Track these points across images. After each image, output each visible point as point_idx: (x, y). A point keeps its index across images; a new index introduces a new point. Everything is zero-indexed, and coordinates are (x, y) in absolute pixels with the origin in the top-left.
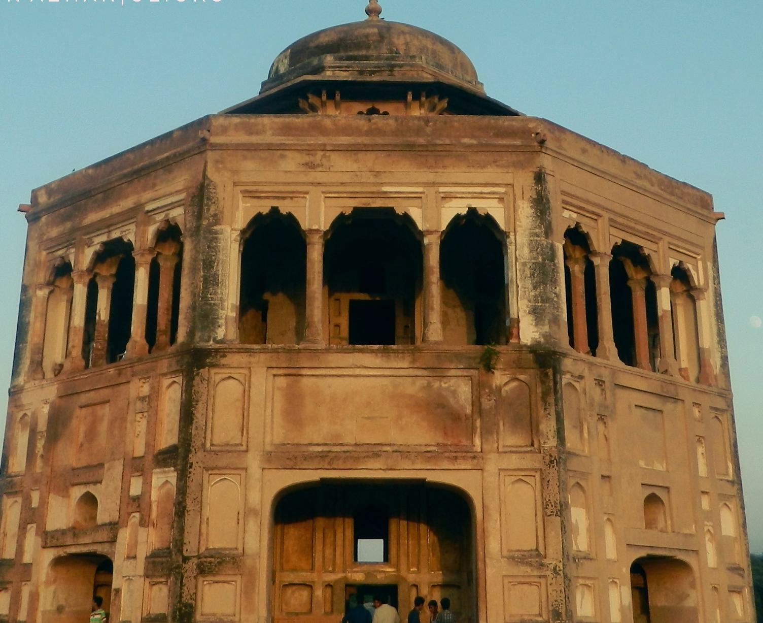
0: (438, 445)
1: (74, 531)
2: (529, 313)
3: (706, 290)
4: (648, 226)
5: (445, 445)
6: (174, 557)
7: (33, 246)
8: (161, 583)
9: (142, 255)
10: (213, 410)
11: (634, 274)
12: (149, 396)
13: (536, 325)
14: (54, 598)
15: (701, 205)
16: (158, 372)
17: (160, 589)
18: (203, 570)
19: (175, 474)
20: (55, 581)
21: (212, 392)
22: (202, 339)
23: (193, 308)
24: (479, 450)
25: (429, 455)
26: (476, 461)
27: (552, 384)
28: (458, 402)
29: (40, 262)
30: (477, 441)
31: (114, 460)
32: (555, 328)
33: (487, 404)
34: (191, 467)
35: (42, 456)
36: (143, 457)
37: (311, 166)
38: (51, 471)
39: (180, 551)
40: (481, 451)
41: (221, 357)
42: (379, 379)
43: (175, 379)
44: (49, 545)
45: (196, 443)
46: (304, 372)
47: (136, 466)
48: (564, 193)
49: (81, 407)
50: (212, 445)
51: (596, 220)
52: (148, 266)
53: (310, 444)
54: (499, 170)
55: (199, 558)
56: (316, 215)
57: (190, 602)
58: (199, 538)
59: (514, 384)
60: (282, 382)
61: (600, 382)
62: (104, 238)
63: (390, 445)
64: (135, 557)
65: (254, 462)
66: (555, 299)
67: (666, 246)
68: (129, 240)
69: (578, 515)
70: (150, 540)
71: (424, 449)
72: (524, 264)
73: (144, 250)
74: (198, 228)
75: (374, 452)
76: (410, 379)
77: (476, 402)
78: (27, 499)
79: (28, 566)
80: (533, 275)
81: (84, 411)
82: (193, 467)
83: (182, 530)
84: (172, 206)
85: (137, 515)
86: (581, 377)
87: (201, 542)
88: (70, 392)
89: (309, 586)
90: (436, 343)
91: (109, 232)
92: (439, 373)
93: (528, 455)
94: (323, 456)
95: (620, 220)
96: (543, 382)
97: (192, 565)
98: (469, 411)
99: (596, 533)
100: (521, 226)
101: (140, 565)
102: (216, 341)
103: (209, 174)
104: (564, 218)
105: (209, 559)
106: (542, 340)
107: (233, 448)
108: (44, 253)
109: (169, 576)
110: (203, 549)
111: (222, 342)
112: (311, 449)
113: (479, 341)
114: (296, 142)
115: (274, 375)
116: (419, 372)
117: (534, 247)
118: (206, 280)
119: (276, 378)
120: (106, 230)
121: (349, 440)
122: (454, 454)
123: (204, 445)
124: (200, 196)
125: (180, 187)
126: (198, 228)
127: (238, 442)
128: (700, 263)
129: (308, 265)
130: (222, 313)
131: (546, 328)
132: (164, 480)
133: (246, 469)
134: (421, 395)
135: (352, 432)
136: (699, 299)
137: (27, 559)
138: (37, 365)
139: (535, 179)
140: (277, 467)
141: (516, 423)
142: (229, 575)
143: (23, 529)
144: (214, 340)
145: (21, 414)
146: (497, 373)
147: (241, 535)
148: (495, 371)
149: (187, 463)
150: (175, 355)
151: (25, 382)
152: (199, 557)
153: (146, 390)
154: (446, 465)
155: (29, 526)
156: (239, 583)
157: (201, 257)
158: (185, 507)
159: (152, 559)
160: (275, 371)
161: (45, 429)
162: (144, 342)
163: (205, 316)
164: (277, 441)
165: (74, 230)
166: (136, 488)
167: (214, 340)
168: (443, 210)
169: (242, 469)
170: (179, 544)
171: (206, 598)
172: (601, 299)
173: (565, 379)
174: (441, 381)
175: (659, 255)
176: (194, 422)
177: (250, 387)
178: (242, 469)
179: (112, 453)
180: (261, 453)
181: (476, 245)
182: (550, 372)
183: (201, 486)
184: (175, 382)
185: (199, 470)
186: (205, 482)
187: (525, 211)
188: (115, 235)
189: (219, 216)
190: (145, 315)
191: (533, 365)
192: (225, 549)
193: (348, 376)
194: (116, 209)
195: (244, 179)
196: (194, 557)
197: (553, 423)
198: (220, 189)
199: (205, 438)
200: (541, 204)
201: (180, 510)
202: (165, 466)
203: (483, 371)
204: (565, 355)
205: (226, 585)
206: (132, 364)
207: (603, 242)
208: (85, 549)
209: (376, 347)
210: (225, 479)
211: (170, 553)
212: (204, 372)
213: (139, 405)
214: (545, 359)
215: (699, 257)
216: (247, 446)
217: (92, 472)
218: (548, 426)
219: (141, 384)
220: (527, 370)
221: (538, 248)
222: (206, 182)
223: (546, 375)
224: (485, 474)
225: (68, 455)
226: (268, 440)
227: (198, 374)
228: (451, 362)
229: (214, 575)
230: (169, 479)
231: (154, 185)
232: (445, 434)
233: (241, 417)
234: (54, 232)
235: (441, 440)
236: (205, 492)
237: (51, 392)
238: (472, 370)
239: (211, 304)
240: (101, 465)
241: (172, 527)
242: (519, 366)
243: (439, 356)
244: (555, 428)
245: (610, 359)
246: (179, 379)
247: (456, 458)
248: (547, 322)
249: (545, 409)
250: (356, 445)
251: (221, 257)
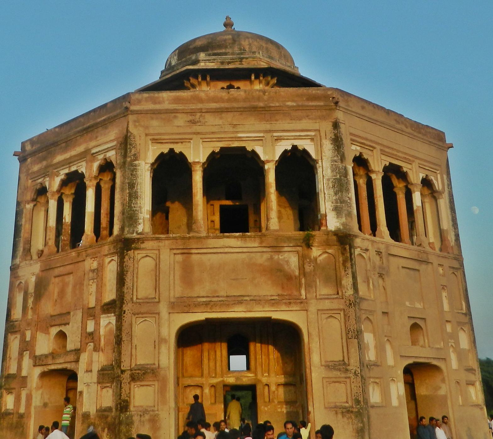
0: (278, 295)
1: (53, 355)
2: (333, 210)
3: (443, 193)
4: (406, 154)
5: (282, 295)
6: (115, 370)
7: (23, 177)
8: (108, 387)
9: (91, 180)
10: (137, 278)
11: (397, 184)
12: (97, 269)
13: (338, 218)
14: (41, 397)
15: (438, 139)
16: (102, 253)
17: (108, 391)
18: (134, 378)
19: (115, 318)
20: (42, 387)
21: (136, 266)
22: (129, 232)
23: (123, 213)
24: (304, 298)
25: (273, 302)
26: (302, 305)
27: (348, 255)
28: (290, 268)
29: (28, 187)
30: (303, 292)
31: (76, 309)
32: (349, 219)
33: (308, 268)
34: (124, 313)
35: (32, 308)
36: (95, 307)
37: (193, 122)
38: (38, 316)
39: (119, 366)
40: (306, 298)
41: (141, 243)
42: (240, 255)
43: (113, 258)
44: (37, 364)
45: (127, 297)
46: (193, 251)
47: (90, 313)
48: (351, 134)
49: (55, 277)
50: (137, 299)
51: (372, 150)
52: (94, 188)
53: (198, 297)
54: (311, 121)
55: (132, 371)
56: (197, 154)
57: (126, 398)
58: (131, 358)
59: (325, 255)
60: (179, 258)
61: (379, 253)
62: (67, 171)
63: (248, 296)
64: (91, 371)
65: (163, 308)
66: (349, 201)
67: (417, 165)
68: (82, 172)
70: (100, 360)
71: (270, 298)
72: (328, 180)
73: (92, 177)
74: (124, 163)
76: (259, 254)
77: (301, 267)
78: (23, 336)
79: (25, 378)
80: (334, 186)
81: (57, 280)
82: (126, 313)
83: (120, 353)
84: (108, 150)
85: (92, 344)
86: (367, 250)
87: (132, 360)
88: (48, 268)
89: (201, 387)
90: (276, 231)
91: (70, 167)
92: (277, 249)
93: (336, 301)
94: (206, 304)
95: (387, 150)
96: (343, 254)
97: (127, 375)
98: (297, 273)
100: (325, 156)
101: (94, 376)
102: (138, 234)
103: (131, 129)
105: (137, 372)
106: (341, 227)
107: (150, 301)
108: (30, 181)
109: (112, 382)
110: (133, 365)
111: (141, 234)
112: (199, 300)
113: (302, 229)
114: (183, 108)
115: (175, 254)
116: (265, 250)
117: (334, 169)
118: (130, 195)
119: (176, 255)
120: (68, 166)
121: (222, 293)
122: (289, 301)
123: (132, 299)
124: (125, 143)
125: (112, 138)
126: (124, 163)
127: (153, 296)
128: (439, 176)
129: (194, 184)
130: (141, 216)
131: (344, 220)
132: (108, 322)
133: (159, 314)
134: (266, 264)
135: (224, 289)
136: (439, 198)
137: (24, 373)
138: (27, 251)
139: (333, 126)
140: (177, 312)
141: (327, 280)
142: (150, 381)
143: (21, 355)
144: (137, 232)
145: (18, 283)
146: (314, 249)
147: (157, 356)
148: (313, 248)
149: (122, 311)
150: (112, 243)
151: (20, 262)
152: (131, 370)
153: (95, 265)
154: (284, 308)
155: (25, 353)
156: (157, 386)
157: (127, 181)
158: (121, 339)
159: (102, 372)
160: (175, 251)
161: (33, 291)
162: (93, 234)
163: (131, 218)
164: (177, 295)
165: (47, 167)
166: (90, 327)
167: (137, 232)
168: (276, 147)
169: (156, 313)
170: (119, 362)
171: (137, 397)
172: (377, 200)
173: (357, 251)
174: (279, 255)
175: (413, 171)
176: (125, 284)
177: (159, 262)
178: (156, 313)
179: (75, 306)
180: (168, 303)
182: (347, 247)
183: (131, 325)
184: (113, 260)
185: (130, 315)
186: (134, 322)
187: (328, 146)
188: (73, 169)
189: (138, 155)
190: (93, 218)
191: (336, 243)
192: (148, 364)
193: (221, 253)
194: (73, 153)
195: (152, 131)
196: (128, 370)
197: (350, 279)
198: (137, 138)
199: (133, 294)
200: (337, 142)
202: (108, 313)
203: (305, 248)
204: (356, 236)
205: (148, 387)
206: (86, 249)
207: (377, 165)
208: (60, 367)
209: (237, 234)
210: (146, 320)
211: (113, 368)
212: (131, 253)
213: (91, 275)
214: (343, 239)
215: (438, 172)
216: (159, 299)
217: (63, 318)
218: (347, 281)
219: (92, 261)
220: (333, 247)
221: (336, 169)
222: (129, 134)
223: (345, 249)
224: (309, 313)
225: (48, 308)
226: (172, 295)
227: (127, 254)
228: (285, 242)
229: (141, 381)
230: (111, 321)
231: (97, 137)
232: (283, 288)
233: (155, 281)
234: (36, 168)
235: (280, 292)
236: (133, 328)
237: (36, 268)
238: (298, 248)
239: (134, 210)
240: (69, 313)
241: (114, 352)
242: (327, 244)
243: (277, 239)
244: (352, 282)
245: (385, 238)
246: (116, 258)
247: (290, 303)
248: (344, 215)
249: (345, 271)
250: (227, 296)
251: (139, 181)
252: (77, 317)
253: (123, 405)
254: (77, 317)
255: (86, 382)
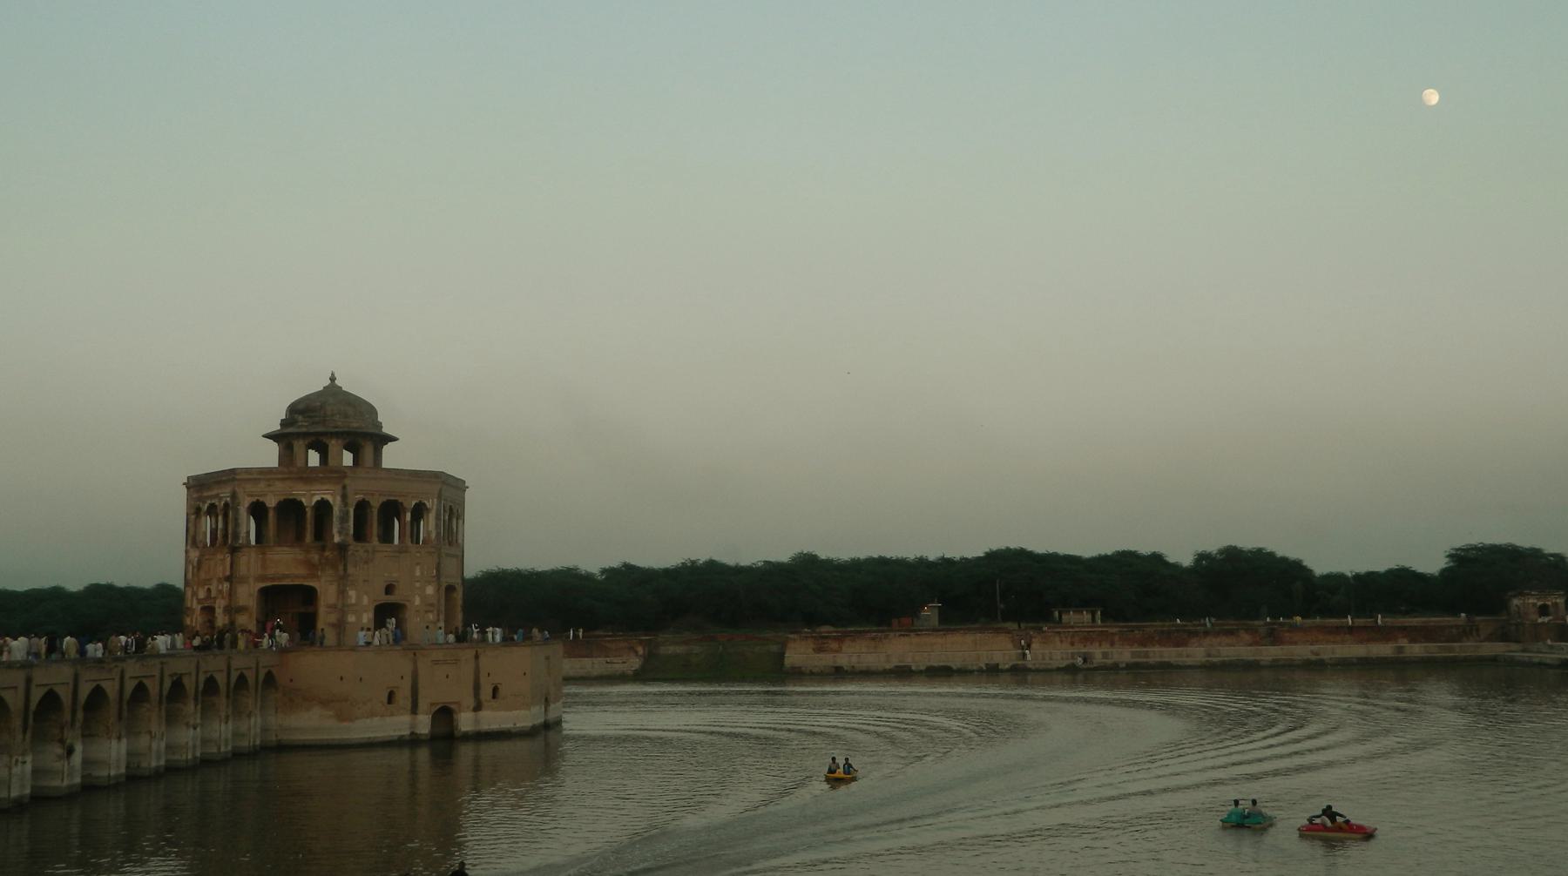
47: (220, 581)
69: (352, 593)
75: (287, 576)
99: (359, 598)
104: (354, 499)
181: (323, 508)
201: (231, 593)
214: (342, 548)
217: (208, 581)
218: (341, 568)
225: (203, 575)
252: (215, 582)
253: (232, 623)
254: (215, 582)
255: (219, 611)
